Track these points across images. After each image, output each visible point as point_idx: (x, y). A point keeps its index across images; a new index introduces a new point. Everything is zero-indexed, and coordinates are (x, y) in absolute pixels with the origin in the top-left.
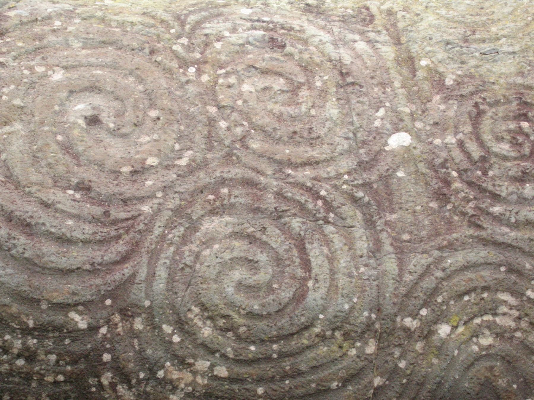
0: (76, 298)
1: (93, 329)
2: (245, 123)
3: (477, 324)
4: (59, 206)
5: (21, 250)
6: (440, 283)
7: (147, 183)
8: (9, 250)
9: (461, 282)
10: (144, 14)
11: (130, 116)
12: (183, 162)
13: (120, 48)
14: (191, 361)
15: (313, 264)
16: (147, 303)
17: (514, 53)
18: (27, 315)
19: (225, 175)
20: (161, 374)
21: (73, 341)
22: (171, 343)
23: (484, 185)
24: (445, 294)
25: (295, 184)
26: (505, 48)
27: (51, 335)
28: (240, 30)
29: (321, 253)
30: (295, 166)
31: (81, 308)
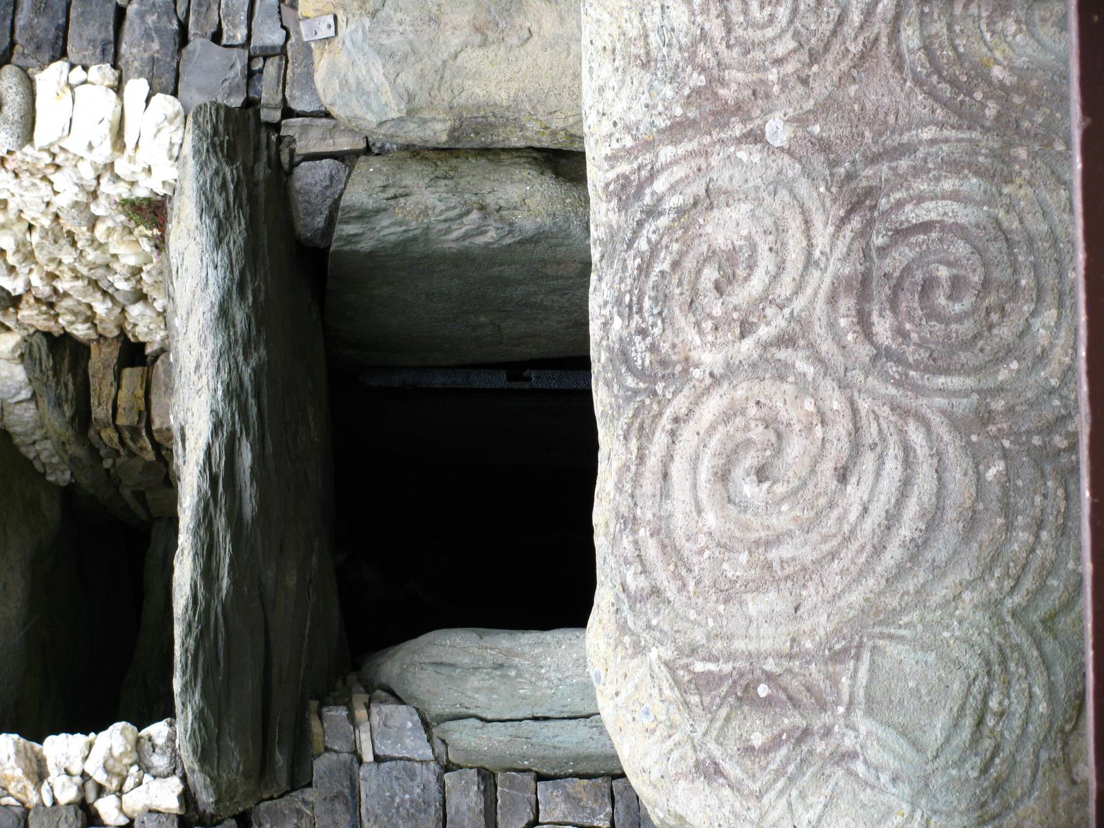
0: (970, 472)
1: (1005, 455)
2: (761, 306)
3: (992, 36)
4: (865, 498)
5: (918, 533)
6: (944, 79)
7: (835, 408)
8: (918, 547)
10: (625, 438)
11: (757, 433)
12: (809, 370)
13: (672, 456)
14: (1039, 350)
15: (926, 218)
16: (975, 397)
17: (662, 7)
18: (991, 525)
19: (824, 322)
20: (1054, 382)
21: (1019, 477)
22: (1018, 371)
23: (828, 33)
24: (957, 73)
25: (833, 246)
26: (657, 18)
27: (1012, 500)
28: (643, 326)
29: (912, 211)
30: (810, 245)
31: (981, 467)
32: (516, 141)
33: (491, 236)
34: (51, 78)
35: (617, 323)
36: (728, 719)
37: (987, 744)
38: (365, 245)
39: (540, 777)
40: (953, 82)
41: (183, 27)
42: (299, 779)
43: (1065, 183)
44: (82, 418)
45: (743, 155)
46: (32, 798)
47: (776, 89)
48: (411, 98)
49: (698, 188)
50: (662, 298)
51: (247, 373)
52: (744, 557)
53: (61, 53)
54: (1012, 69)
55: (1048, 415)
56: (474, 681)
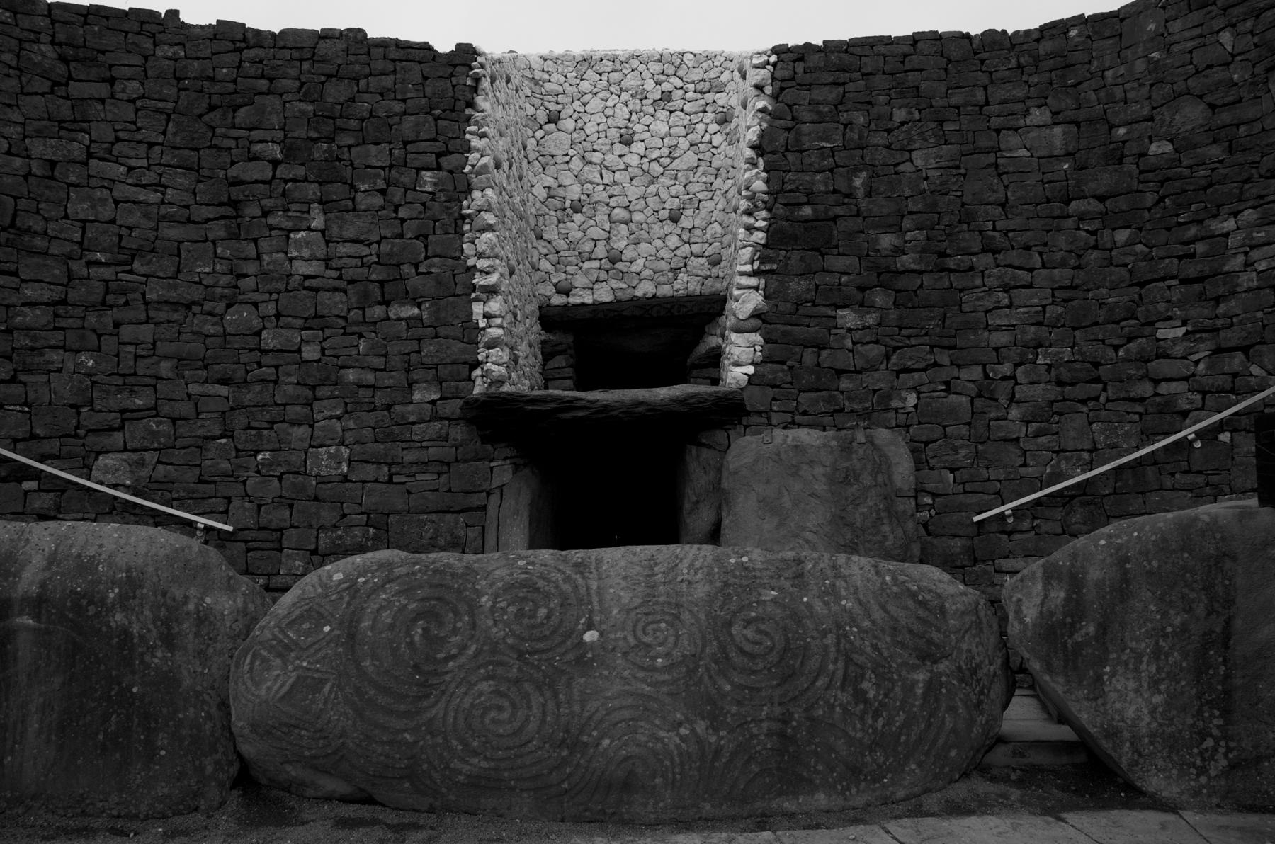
1: (416, 742)
9: (617, 716)
32: (724, 514)
33: (687, 506)
34: (757, 338)
35: (521, 563)
36: (318, 612)
37: (285, 730)
38: (688, 458)
39: (483, 527)
40: (601, 721)
41: (778, 387)
42: (485, 440)
43: (551, 773)
44: (695, 366)
45: (583, 621)
46: (480, 345)
47: (612, 636)
48: (736, 473)
49: (573, 600)
50: (523, 584)
51: (616, 413)
52: (389, 621)
53: (767, 341)
54: (606, 749)
55: (436, 762)
56: (513, 502)
